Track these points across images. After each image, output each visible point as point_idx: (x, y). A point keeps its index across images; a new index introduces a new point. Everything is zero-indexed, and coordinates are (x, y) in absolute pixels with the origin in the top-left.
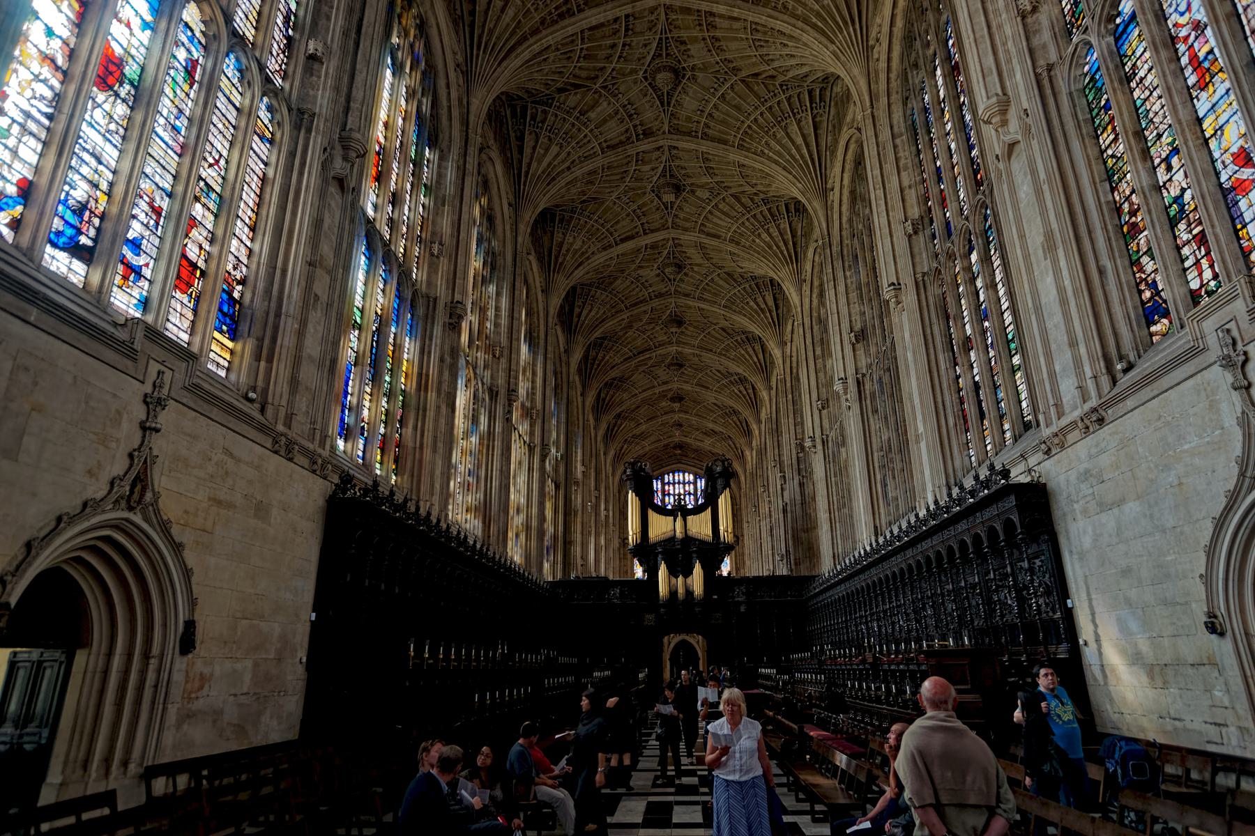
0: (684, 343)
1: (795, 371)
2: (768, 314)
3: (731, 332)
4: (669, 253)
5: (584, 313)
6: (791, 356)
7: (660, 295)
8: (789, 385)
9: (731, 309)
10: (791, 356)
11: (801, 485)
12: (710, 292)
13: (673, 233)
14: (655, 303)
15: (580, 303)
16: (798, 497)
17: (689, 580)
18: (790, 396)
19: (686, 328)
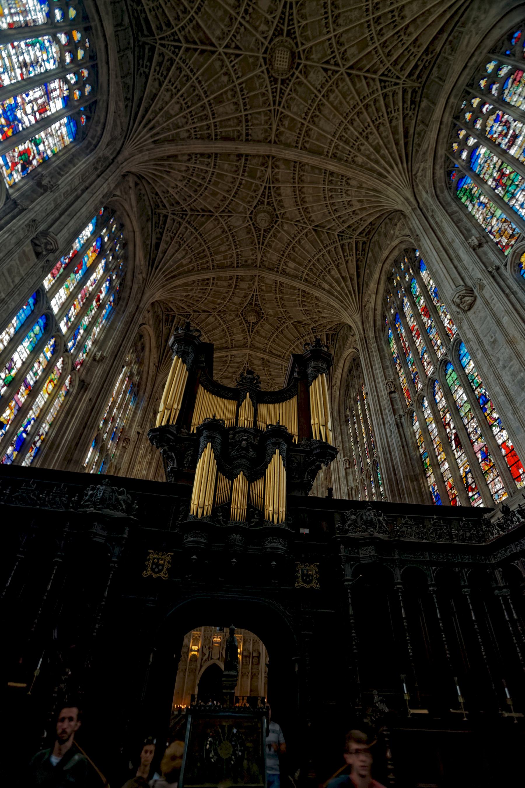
0: (258, 348)
1: (379, 323)
2: (349, 283)
3: (302, 330)
4: (263, 194)
5: (171, 251)
6: (375, 309)
7: (246, 266)
8: (371, 335)
9: (311, 283)
10: (375, 309)
11: (399, 426)
12: (294, 260)
13: (274, 151)
14: (241, 272)
15: (168, 239)
16: (395, 441)
17: (258, 484)
18: (374, 346)
19: (262, 327)
